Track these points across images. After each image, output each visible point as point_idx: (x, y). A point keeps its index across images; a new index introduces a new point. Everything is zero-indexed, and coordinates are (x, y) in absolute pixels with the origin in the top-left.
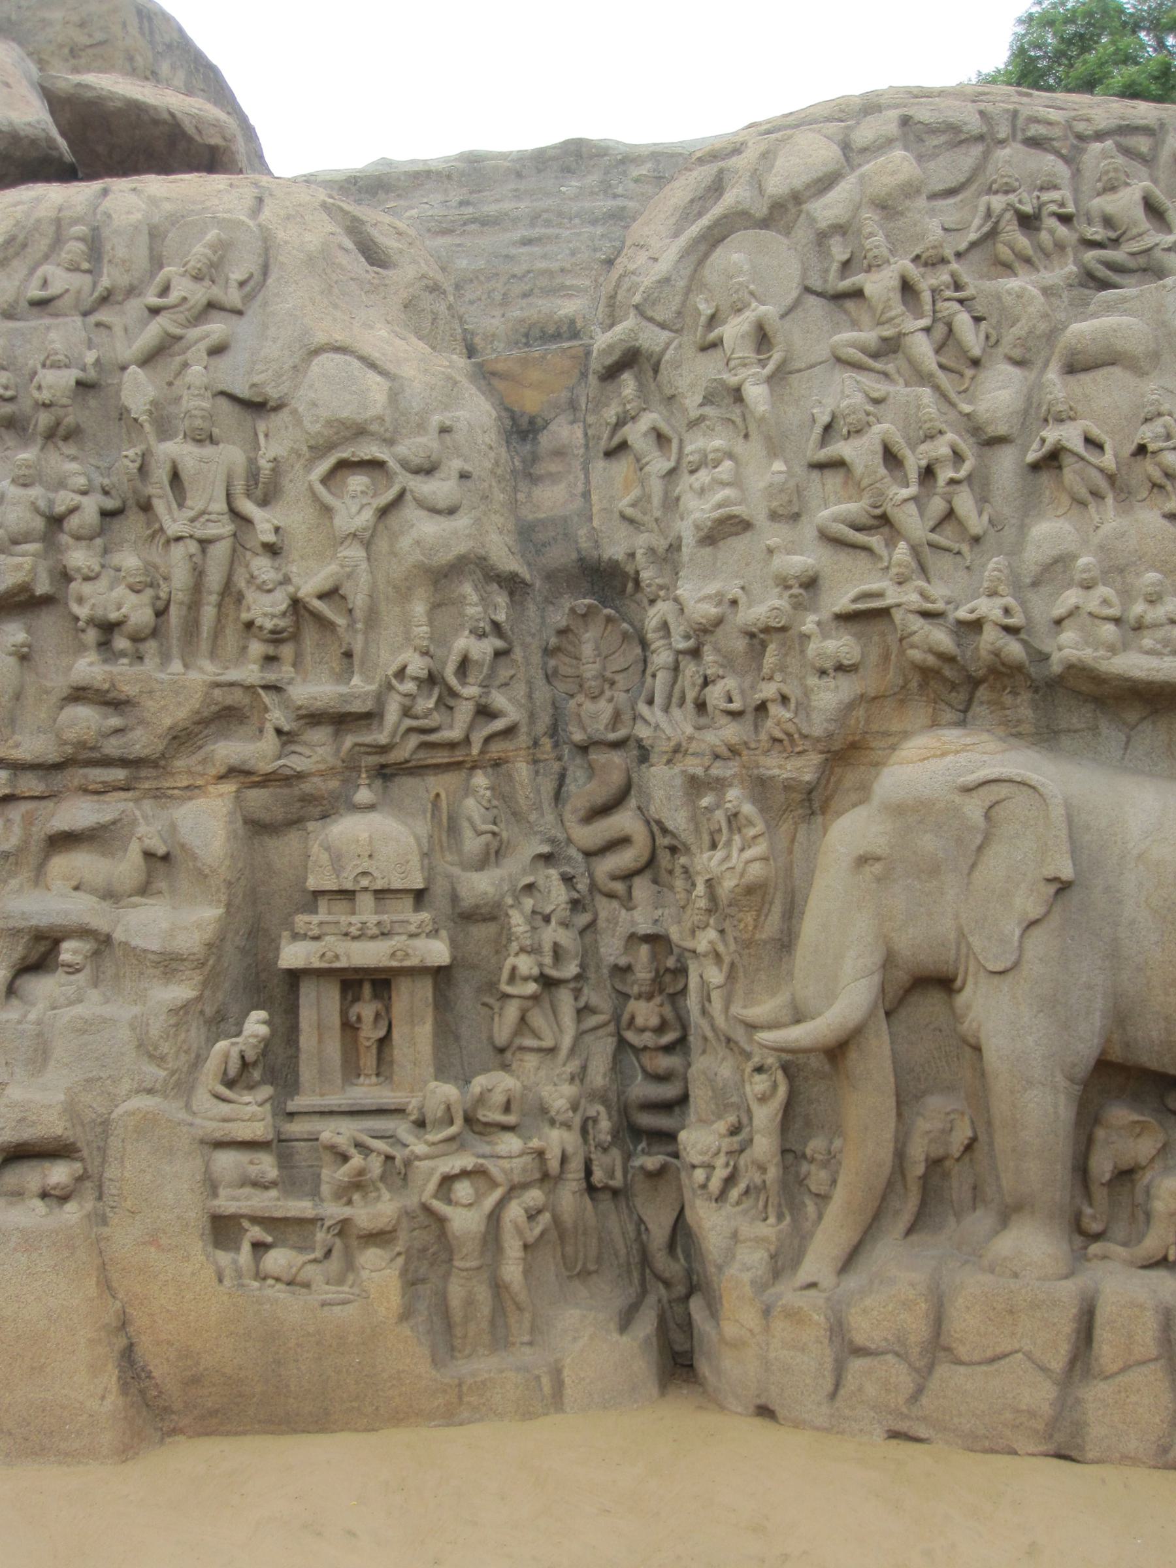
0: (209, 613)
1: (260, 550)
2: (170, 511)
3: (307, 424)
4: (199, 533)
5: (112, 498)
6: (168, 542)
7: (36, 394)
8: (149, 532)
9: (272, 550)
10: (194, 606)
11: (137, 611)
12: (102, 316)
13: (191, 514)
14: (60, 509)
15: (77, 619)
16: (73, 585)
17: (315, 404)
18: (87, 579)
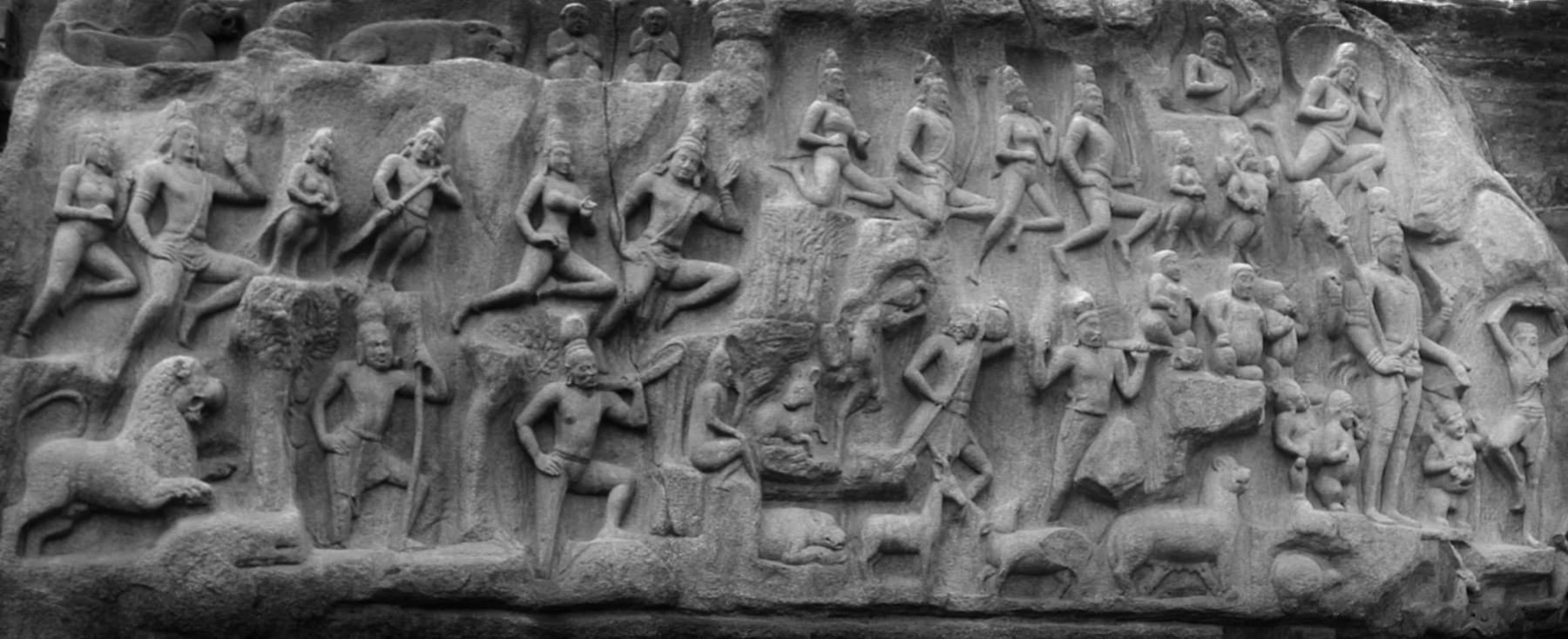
0: (1401, 455)
1: (1451, 393)
2: (1378, 341)
3: (1486, 259)
4: (1409, 371)
5: (1297, 321)
6: (1357, 376)
7: (1238, 198)
8: (1335, 363)
9: (1461, 391)
10: (1392, 448)
11: (1345, 448)
12: (1254, 118)
13: (1401, 348)
14: (1275, 329)
15: (1294, 456)
16: (1285, 416)
17: (1491, 242)
18: (1300, 410)
